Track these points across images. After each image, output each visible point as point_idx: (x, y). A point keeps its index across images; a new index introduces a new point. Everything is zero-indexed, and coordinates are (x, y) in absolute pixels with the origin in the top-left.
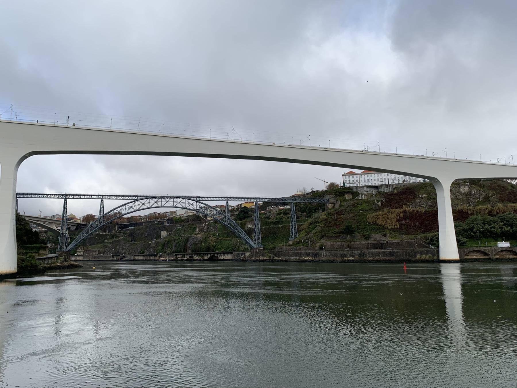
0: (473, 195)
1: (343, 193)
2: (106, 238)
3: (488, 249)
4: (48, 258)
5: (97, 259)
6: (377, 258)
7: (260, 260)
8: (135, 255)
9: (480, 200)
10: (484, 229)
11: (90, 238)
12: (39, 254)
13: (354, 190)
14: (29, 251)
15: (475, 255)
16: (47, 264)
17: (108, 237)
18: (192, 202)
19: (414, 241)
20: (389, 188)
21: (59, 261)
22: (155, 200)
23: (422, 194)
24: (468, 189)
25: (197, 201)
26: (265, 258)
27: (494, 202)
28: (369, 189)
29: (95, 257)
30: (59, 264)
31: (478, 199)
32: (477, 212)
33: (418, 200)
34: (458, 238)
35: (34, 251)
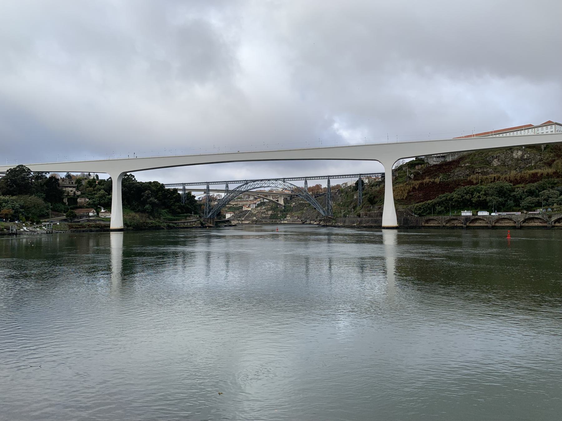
0: (526, 159)
1: (413, 165)
2: (306, 206)
3: (440, 218)
4: (187, 222)
5: (294, 223)
6: (368, 224)
7: (326, 225)
8: (311, 220)
9: (533, 165)
10: (463, 199)
11: (295, 206)
12: (186, 220)
13: (425, 161)
14: (180, 218)
15: (433, 223)
16: (187, 225)
17: (307, 205)
18: (280, 182)
19: (404, 210)
20: (454, 157)
21: (196, 224)
22: (257, 182)
23: (465, 164)
24: (521, 153)
25: (284, 182)
26: (330, 224)
27: (539, 167)
28: (438, 159)
29: (293, 221)
30: (194, 226)
31: (530, 164)
32: (481, 182)
33: (458, 169)
34: (125, 217)
35: (183, 218)
